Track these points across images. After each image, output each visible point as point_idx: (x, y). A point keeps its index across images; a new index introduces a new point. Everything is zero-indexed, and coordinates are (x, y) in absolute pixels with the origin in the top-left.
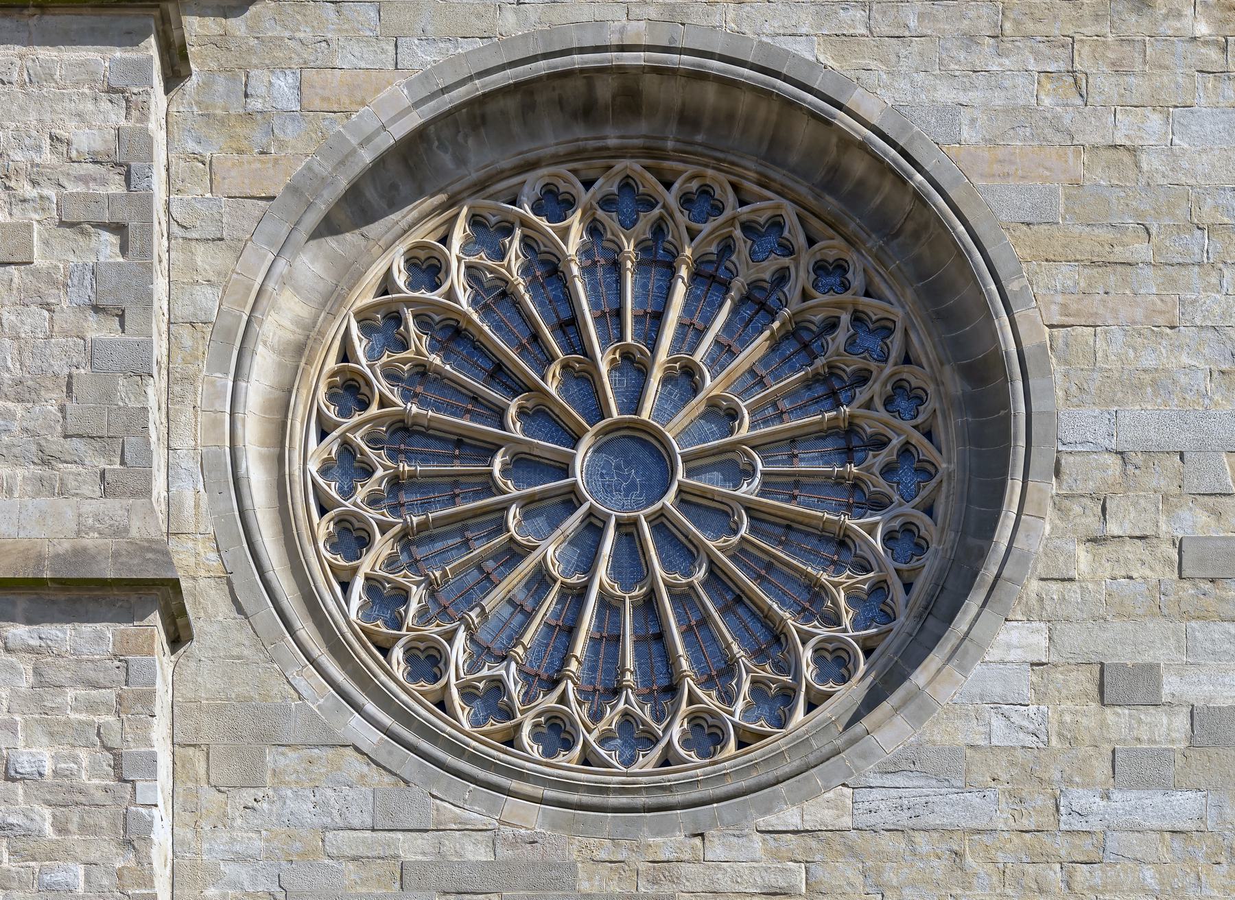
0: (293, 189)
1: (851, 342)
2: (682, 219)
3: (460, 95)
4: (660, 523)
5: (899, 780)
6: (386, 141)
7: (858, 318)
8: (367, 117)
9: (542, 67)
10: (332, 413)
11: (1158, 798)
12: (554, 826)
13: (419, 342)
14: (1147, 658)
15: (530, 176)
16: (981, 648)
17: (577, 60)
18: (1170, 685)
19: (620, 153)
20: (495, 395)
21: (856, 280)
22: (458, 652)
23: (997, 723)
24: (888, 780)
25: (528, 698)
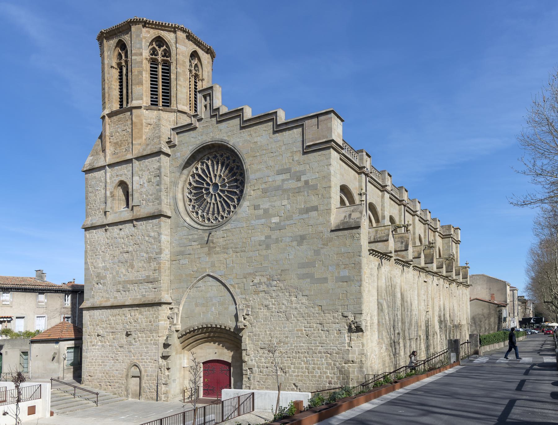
5: (235, 222)
11: (260, 220)
16: (242, 205)
18: (261, 207)
24: (234, 223)
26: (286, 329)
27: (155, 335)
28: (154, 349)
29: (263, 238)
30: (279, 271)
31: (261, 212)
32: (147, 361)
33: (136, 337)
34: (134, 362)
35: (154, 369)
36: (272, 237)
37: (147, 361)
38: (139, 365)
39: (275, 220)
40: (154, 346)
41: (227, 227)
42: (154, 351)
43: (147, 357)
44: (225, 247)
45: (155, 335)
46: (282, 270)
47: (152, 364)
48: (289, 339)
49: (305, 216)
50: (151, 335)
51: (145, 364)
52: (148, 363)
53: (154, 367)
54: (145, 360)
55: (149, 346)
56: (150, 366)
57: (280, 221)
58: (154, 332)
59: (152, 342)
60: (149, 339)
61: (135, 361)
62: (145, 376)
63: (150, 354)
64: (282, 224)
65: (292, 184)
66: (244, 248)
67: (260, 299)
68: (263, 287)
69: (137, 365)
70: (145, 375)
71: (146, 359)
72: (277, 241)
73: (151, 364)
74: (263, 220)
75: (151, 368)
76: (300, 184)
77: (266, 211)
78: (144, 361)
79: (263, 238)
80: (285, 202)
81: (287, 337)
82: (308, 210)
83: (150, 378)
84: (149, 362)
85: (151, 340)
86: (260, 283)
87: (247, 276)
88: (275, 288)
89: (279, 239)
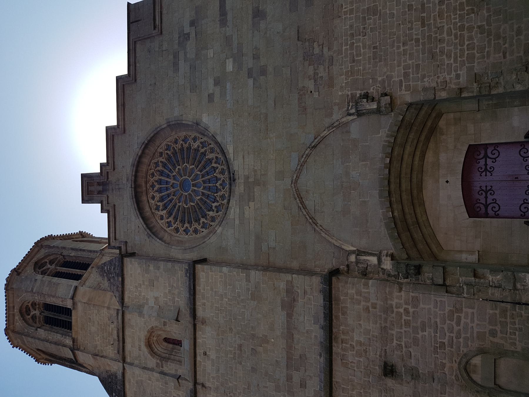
0: (149, 238)
1: (170, 151)
2: (154, 178)
3: (138, 212)
4: (193, 180)
5: (226, 137)
6: (143, 223)
7: (166, 150)
8: (141, 226)
9: (134, 199)
10: (179, 233)
12: (234, 197)
13: (171, 219)
14: (207, 97)
15: (150, 201)
17: (133, 194)
18: (211, 91)
19: (146, 187)
20: (177, 207)
21: (161, 151)
22: (211, 213)
23: (217, 121)
24: (226, 138)
25: (218, 202)
26: (395, 12)
27: (396, 300)
28: (427, 307)
29: (251, 82)
30: (300, 43)
31: (218, 90)
32: (456, 328)
33: (399, 353)
34: (459, 368)
35: (475, 311)
36: (250, 65)
37: (456, 328)
38: (465, 355)
39: (230, 66)
40: (422, 306)
41: (230, 149)
42: (432, 306)
43: (446, 327)
44: (256, 154)
45: (396, 300)
46: (298, 40)
47: (463, 315)
48: (413, 3)
49: (229, 17)
50: (395, 310)
51: (463, 336)
52: (461, 327)
53: (470, 311)
54: (454, 335)
55: (420, 320)
56: (469, 321)
57: (231, 57)
58: (389, 302)
59: (411, 310)
60: (404, 317)
61: (456, 366)
62: (495, 340)
63: (438, 320)
64: (235, 51)
65: (191, 46)
66: (262, 116)
67: (341, 75)
68: (322, 72)
69: (464, 360)
70: (491, 338)
71: (452, 332)
72: (256, 57)
73: (463, 320)
74: (228, 86)
75: (472, 321)
76: (193, 35)
77: (217, 83)
78: (454, 338)
79: (251, 82)
80: (210, 53)
81: (410, 7)
82: (223, 13)
83: (499, 326)
84: (458, 324)
85: (406, 311)
86: (315, 78)
87: (303, 104)
88: (325, 50)
89: (254, 53)
